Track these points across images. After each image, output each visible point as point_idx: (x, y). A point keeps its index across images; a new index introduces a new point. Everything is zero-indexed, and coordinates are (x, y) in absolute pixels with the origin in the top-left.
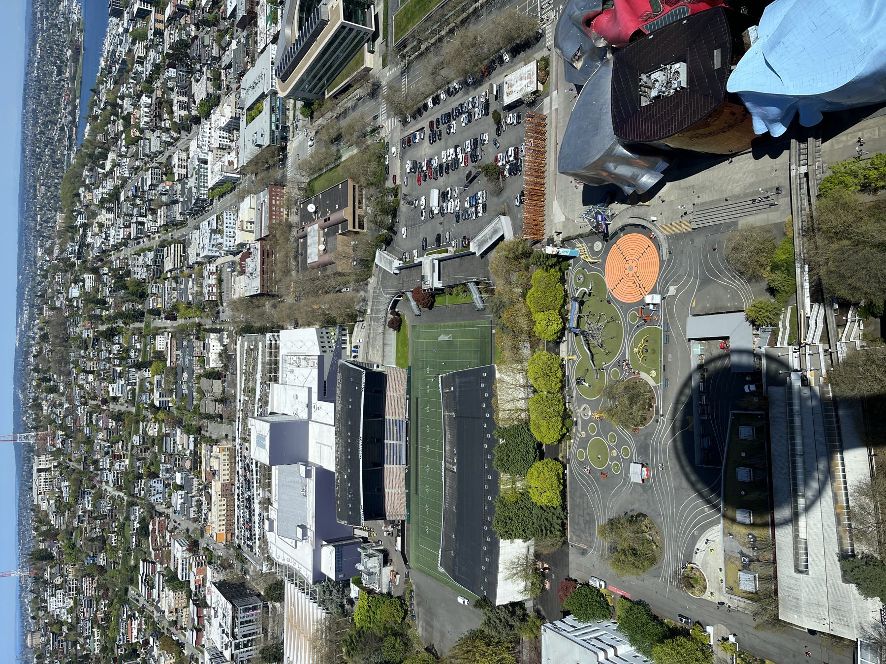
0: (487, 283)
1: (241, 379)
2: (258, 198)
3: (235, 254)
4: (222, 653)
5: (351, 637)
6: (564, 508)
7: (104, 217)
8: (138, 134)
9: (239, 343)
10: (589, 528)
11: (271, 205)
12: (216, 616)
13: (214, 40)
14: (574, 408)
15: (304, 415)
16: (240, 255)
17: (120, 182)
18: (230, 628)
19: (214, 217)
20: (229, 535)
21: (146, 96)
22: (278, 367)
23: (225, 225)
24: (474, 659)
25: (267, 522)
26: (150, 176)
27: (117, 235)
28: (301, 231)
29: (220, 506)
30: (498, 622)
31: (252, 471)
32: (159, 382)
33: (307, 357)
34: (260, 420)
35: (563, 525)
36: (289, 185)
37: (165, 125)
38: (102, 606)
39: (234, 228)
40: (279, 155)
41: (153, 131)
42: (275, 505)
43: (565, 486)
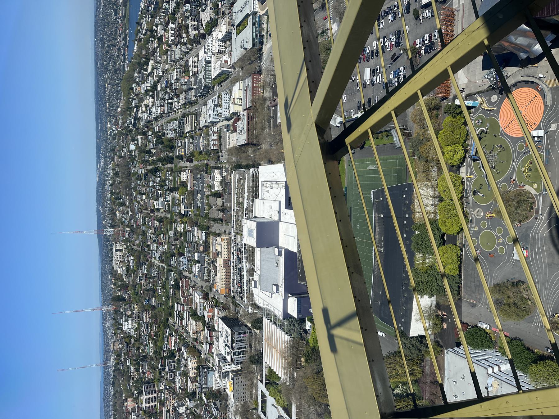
0: (405, 129)
1: (234, 197)
2: (245, 83)
3: (229, 120)
4: (225, 357)
5: (308, 352)
6: (460, 276)
7: (148, 101)
8: (167, 48)
9: (232, 175)
10: (479, 290)
11: (253, 87)
12: (222, 336)
14: (470, 211)
15: (276, 218)
16: (232, 120)
17: (157, 79)
18: (230, 343)
19: (216, 96)
20: (227, 290)
21: (172, 23)
22: (259, 190)
23: (223, 101)
24: (395, 368)
25: (253, 282)
26: (175, 74)
27: (156, 111)
28: (273, 102)
29: (222, 273)
30: (411, 346)
31: (242, 252)
32: (183, 199)
33: (277, 182)
34: (250, 220)
35: (459, 287)
36: (264, 72)
37: (184, 41)
38: (154, 328)
39: (228, 103)
40: (258, 54)
41: (177, 45)
42: (258, 272)
43: (461, 262)
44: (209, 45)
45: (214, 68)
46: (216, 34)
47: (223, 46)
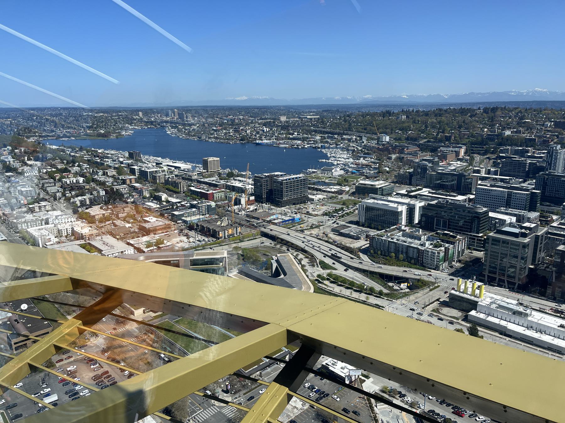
8: (57, 178)
13: (128, 213)
21: (83, 180)
26: (28, 189)
37: (67, 193)
41: (61, 187)
44: (66, 219)
45: (39, 229)
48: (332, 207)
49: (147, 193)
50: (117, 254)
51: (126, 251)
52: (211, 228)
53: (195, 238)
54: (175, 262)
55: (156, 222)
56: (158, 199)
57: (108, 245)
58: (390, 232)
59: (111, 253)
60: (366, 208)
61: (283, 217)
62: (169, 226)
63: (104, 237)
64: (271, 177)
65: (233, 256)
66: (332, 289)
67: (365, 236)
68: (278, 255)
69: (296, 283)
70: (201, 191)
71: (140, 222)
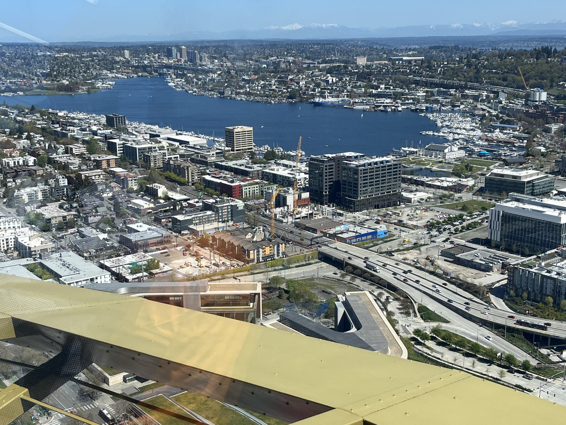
13: (103, 216)
21: (35, 160)
37: (9, 182)
44: (7, 223)
46: (25, 232)
47: (7, 246)
48: (442, 213)
49: (133, 184)
50: (85, 282)
51: (99, 278)
52: (236, 244)
53: (210, 260)
54: (176, 298)
55: (148, 231)
56: (152, 194)
57: (71, 267)
58: (544, 259)
59: (74, 281)
60: (503, 216)
61: (358, 229)
62: (169, 239)
63: (64, 253)
64: (338, 160)
65: (271, 292)
66: (439, 356)
67: (500, 265)
68: (348, 293)
69: (377, 343)
70: (221, 183)
71: (122, 231)
